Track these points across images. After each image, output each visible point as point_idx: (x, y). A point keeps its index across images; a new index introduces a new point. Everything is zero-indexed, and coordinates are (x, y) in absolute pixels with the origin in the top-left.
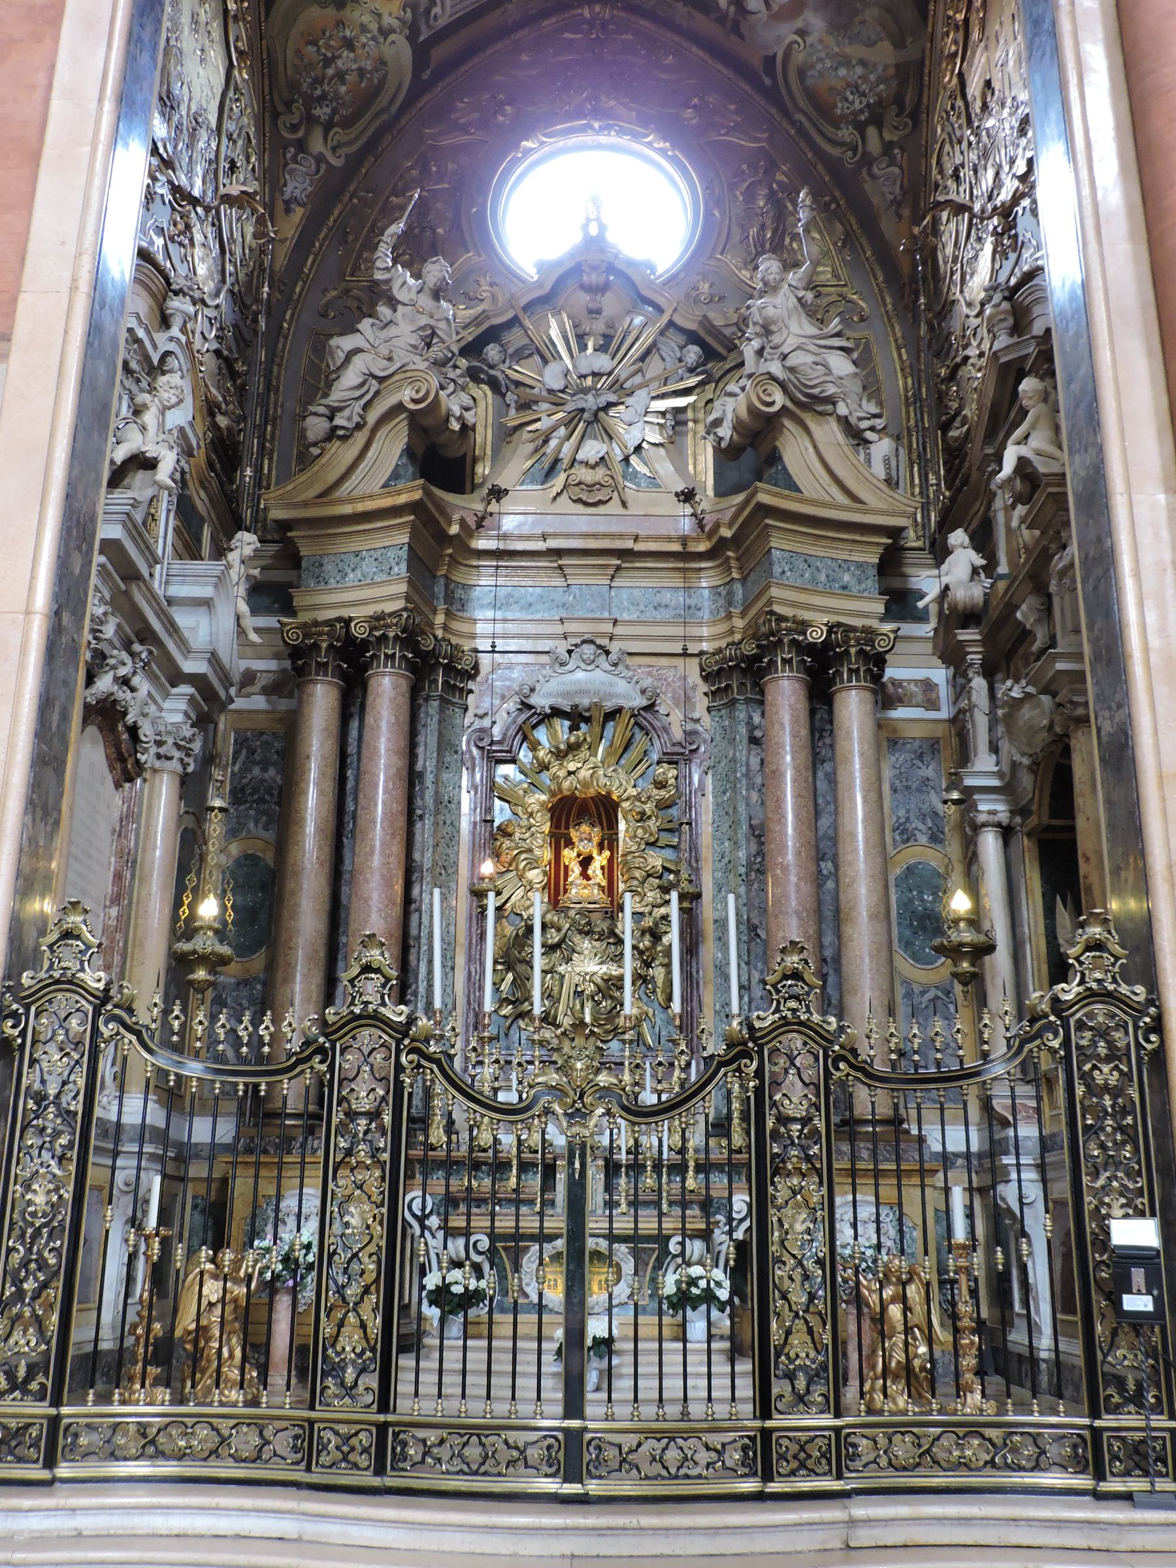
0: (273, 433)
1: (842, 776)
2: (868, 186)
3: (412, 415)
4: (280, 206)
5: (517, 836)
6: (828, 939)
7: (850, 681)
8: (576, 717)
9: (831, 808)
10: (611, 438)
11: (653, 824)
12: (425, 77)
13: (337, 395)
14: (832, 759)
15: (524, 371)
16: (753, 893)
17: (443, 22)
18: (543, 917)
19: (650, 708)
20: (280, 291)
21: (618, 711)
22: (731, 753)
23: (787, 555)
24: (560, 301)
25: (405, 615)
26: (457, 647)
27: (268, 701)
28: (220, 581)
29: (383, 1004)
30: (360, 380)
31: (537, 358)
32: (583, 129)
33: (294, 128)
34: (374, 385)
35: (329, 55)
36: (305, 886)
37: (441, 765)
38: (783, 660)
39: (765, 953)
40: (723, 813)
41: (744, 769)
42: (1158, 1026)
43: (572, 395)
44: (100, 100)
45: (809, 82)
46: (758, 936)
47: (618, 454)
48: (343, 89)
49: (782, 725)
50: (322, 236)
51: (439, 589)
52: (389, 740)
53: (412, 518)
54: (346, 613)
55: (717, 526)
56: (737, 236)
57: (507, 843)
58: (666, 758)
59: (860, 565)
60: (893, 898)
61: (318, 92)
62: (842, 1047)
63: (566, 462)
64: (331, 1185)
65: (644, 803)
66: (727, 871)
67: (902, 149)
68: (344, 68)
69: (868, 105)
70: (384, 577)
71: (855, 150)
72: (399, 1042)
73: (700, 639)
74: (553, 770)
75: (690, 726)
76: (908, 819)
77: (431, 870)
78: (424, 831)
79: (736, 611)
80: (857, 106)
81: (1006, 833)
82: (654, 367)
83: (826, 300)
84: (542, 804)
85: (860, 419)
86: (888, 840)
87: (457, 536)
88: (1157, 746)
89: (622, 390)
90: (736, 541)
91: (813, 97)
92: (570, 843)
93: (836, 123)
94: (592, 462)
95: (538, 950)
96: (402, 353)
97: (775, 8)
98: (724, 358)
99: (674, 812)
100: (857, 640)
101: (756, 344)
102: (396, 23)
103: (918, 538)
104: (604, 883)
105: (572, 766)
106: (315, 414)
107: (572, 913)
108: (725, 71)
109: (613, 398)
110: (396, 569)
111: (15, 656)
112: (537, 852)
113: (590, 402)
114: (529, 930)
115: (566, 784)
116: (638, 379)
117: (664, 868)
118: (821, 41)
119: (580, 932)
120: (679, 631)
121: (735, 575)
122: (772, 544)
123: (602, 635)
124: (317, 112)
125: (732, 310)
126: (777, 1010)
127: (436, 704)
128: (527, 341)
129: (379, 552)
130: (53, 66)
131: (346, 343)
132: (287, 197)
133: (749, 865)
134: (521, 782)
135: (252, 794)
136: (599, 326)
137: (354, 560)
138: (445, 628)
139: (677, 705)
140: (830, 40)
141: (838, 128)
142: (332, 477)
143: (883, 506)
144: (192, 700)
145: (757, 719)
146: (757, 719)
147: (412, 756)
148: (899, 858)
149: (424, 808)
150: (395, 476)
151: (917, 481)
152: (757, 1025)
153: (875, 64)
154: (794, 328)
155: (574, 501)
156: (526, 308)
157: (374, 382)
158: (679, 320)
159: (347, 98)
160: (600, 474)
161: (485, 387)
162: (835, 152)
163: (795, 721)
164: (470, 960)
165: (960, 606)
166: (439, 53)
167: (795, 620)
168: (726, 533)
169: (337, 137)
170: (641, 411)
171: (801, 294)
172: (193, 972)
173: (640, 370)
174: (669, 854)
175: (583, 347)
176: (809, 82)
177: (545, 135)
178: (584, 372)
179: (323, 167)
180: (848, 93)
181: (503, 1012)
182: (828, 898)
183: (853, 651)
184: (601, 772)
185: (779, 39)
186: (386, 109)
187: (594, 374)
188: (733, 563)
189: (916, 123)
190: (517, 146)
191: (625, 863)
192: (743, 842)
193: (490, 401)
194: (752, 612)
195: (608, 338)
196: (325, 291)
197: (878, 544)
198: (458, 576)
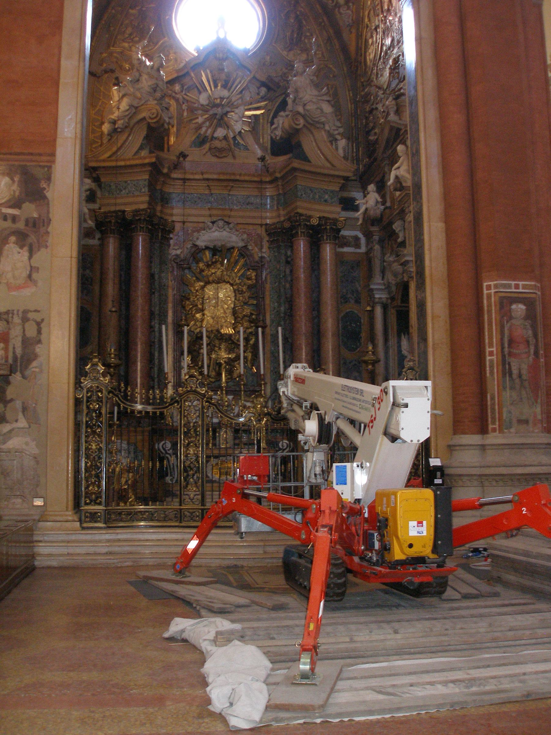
2: (338, 16)
5: (192, 299)
7: (327, 240)
8: (215, 251)
10: (228, 127)
11: (247, 295)
15: (192, 95)
22: (278, 267)
25: (149, 211)
29: (197, 387)
31: (196, 90)
38: (301, 232)
43: (212, 107)
47: (231, 135)
49: (300, 259)
54: (122, 208)
57: (187, 302)
59: (332, 192)
60: (340, 325)
63: (210, 137)
65: (243, 286)
73: (266, 218)
85: (334, 130)
88: (432, 306)
90: (283, 178)
105: (213, 271)
109: (229, 109)
110: (143, 190)
113: (219, 111)
119: (218, 339)
123: (225, 216)
127: (158, 245)
133: (285, 313)
136: (223, 77)
138: (161, 212)
139: (256, 246)
145: (289, 253)
146: (289, 253)
151: (355, 150)
160: (224, 144)
163: (305, 257)
168: (278, 175)
170: (241, 115)
171: (312, 78)
175: (216, 86)
178: (216, 97)
184: (225, 273)
188: (280, 187)
196: (101, 53)
197: (339, 183)
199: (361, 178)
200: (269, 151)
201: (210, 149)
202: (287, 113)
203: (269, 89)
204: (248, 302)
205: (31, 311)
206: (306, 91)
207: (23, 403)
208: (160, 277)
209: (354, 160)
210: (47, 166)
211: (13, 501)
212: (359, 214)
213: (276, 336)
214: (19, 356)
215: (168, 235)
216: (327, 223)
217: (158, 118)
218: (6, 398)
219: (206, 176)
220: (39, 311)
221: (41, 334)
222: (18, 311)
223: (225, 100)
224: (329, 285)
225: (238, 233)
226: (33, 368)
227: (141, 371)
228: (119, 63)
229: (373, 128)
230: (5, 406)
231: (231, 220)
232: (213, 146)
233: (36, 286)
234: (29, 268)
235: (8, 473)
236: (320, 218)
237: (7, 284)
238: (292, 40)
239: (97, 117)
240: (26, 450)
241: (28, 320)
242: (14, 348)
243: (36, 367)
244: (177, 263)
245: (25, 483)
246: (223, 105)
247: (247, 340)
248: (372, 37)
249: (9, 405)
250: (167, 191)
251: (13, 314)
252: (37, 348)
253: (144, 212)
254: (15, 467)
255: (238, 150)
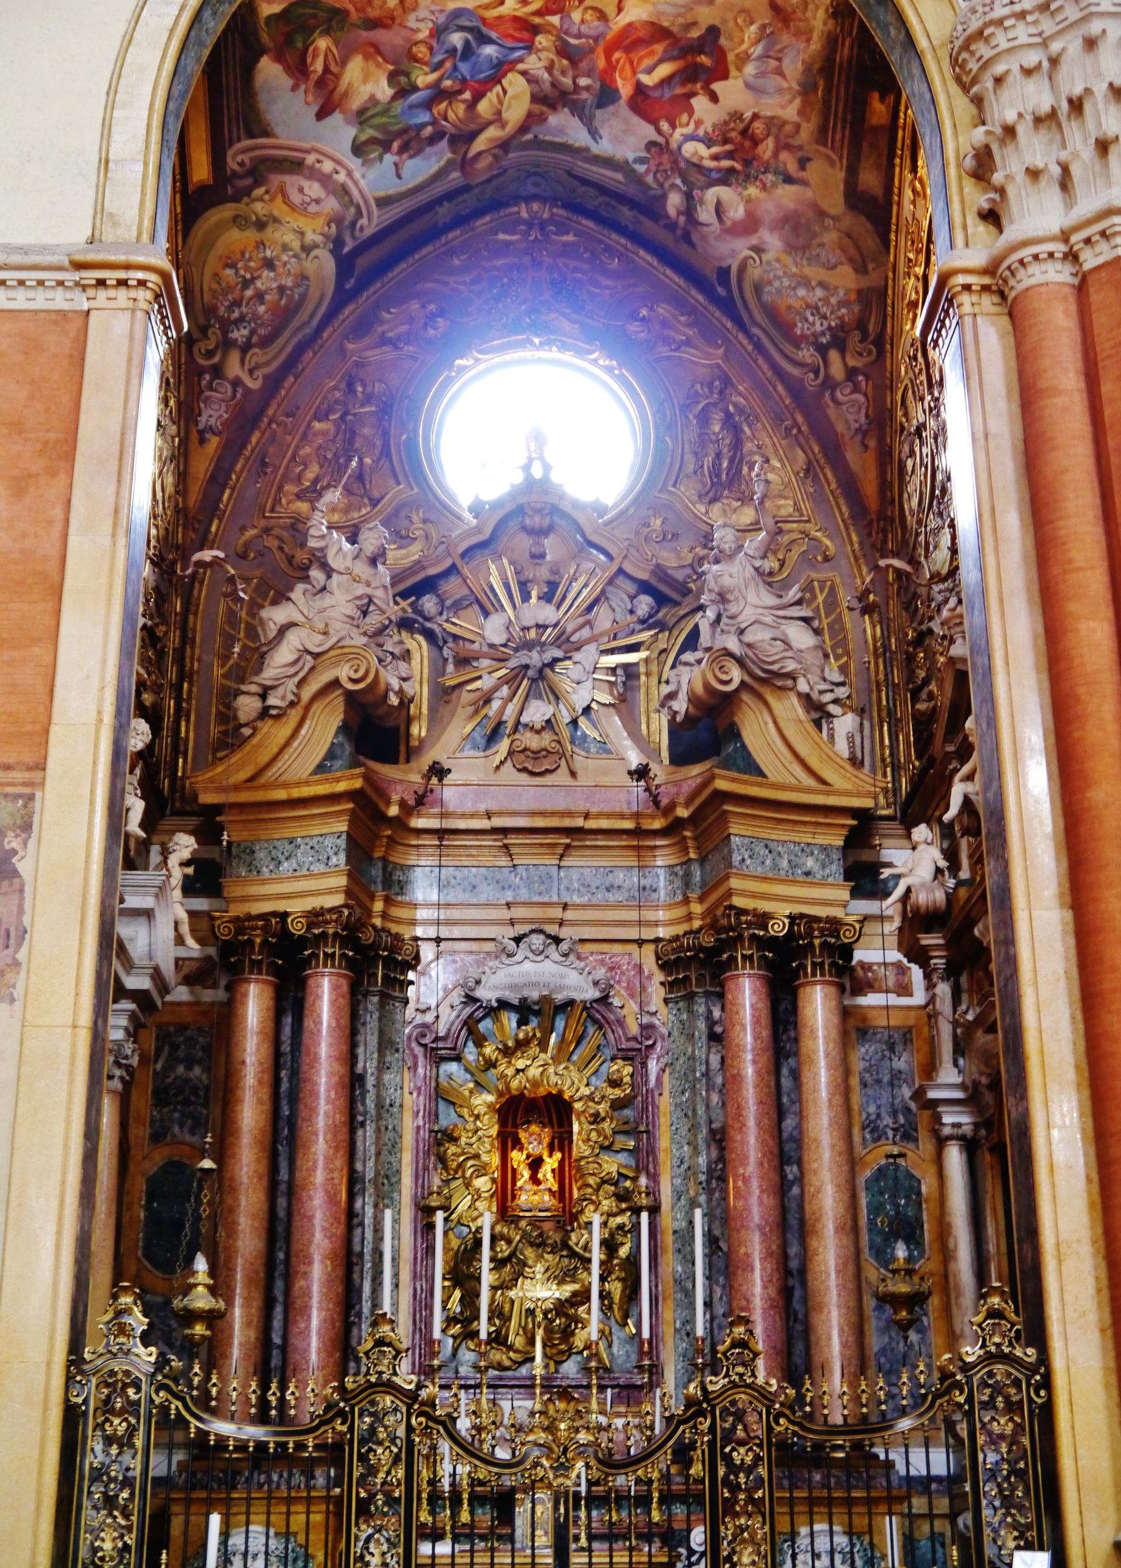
0: (190, 691)
1: (806, 1077)
2: (832, 411)
3: (350, 696)
4: (194, 437)
5: (463, 1140)
6: (793, 1250)
7: (814, 974)
8: (524, 1010)
9: (796, 1107)
10: (557, 698)
11: (608, 1127)
12: (348, 286)
13: (268, 674)
14: (796, 1054)
15: (464, 624)
16: (714, 1203)
17: (369, 232)
18: (492, 1228)
19: (604, 1000)
20: (194, 530)
21: (571, 1003)
22: (690, 1050)
23: (747, 841)
24: (502, 544)
25: (346, 912)
26: (397, 937)
27: (192, 993)
28: (161, 891)
30: (295, 656)
31: (476, 607)
32: (521, 345)
33: (210, 354)
34: (309, 661)
35: (248, 276)
36: (243, 1201)
37: (382, 1067)
39: (727, 1266)
40: (679, 1113)
41: (704, 1068)
42: (1047, 1383)
43: (516, 650)
44: (114, 535)
45: (766, 298)
46: (720, 1249)
47: (566, 717)
48: (262, 309)
49: (743, 1026)
50: (238, 467)
51: (377, 872)
52: (330, 1045)
53: (351, 806)
54: (281, 906)
55: (672, 806)
56: (690, 467)
57: (452, 1149)
58: (620, 1054)
59: (824, 849)
60: (863, 1201)
61: (236, 315)
62: (782, 1404)
63: (510, 725)
64: (354, 1530)
65: (599, 1103)
66: (686, 1178)
67: (867, 378)
68: (263, 288)
69: (830, 328)
70: (322, 868)
71: (817, 373)
72: (409, 1407)
73: (656, 924)
74: (502, 1068)
75: (646, 1020)
76: (878, 1116)
77: (375, 1181)
78: (367, 1138)
79: (693, 896)
80: (818, 328)
81: (970, 1146)
82: (603, 619)
83: (785, 539)
84: (490, 1106)
85: (821, 692)
86: (857, 1138)
87: (396, 819)
89: (568, 645)
90: (693, 819)
91: (771, 313)
92: (518, 1144)
93: (796, 342)
94: (538, 726)
95: (486, 1264)
96: (338, 625)
97: (729, 223)
98: (677, 604)
99: (627, 1112)
100: (822, 930)
101: (711, 614)
102: (319, 239)
103: (888, 806)
104: (555, 1188)
105: (520, 1064)
106: (248, 693)
107: (523, 1224)
108: (676, 278)
109: (559, 653)
110: (334, 860)
111: (65, 1067)
112: (485, 1158)
113: (535, 658)
114: (478, 1243)
115: (514, 1084)
116: (585, 633)
117: (619, 1174)
118: (778, 260)
119: (532, 1244)
120: (633, 915)
121: (692, 855)
122: (732, 831)
123: (551, 921)
124: (235, 335)
125: (686, 550)
126: (727, 1375)
127: (375, 999)
128: (466, 592)
129: (315, 840)
130: (69, 501)
131: (276, 615)
132: (201, 426)
133: (710, 1172)
134: (466, 1081)
135: (176, 1095)
136: (543, 573)
137: (290, 848)
138: (384, 916)
139: (632, 996)
140: (788, 260)
141: (798, 348)
142: (264, 757)
143: (848, 786)
144: (133, 1016)
146: (717, 1013)
147: (351, 1058)
148: (869, 1158)
149: (365, 1113)
150: (331, 755)
151: (887, 742)
152: (710, 1388)
153: (836, 288)
154: (752, 598)
155: (519, 770)
156: (463, 555)
157: (309, 658)
158: (628, 568)
159: (266, 317)
160: (546, 740)
161: (420, 638)
162: (795, 372)
163: (756, 1021)
164: (415, 1277)
165: (923, 909)
166: (362, 263)
167: (754, 912)
168: (683, 812)
169: (255, 359)
171: (758, 563)
172: (191, 1327)
173: (589, 623)
174: (623, 1158)
175: (526, 597)
176: (766, 298)
177: (480, 352)
178: (527, 624)
179: (240, 390)
180: (808, 314)
181: (452, 1332)
182: (793, 1205)
183: (817, 942)
184: (551, 1070)
185: (734, 253)
186: (308, 322)
187: (538, 626)
188: (690, 843)
189: (881, 353)
190: (452, 365)
191: (579, 1169)
192: (702, 1147)
193: (425, 654)
194: (713, 898)
195: (553, 585)
196: (243, 529)
197: (843, 826)
198: (396, 858)
199: (904, 811)
200: (665, 754)
201: (511, 753)
202: (699, 654)
203: (661, 600)
204: (612, 1144)
206: (745, 598)
208: (378, 1085)
209: (885, 767)
210: (21, 796)
212: (890, 905)
213: (685, 1237)
215: (404, 972)
216: (813, 930)
217: (369, 680)
219: (498, 822)
223: (549, 630)
224: (824, 1094)
225: (582, 964)
227: (319, 1333)
228: (286, 549)
229: (926, 682)
231: (565, 932)
232: (519, 746)
236: (792, 918)
238: (718, 476)
239: (228, 683)
244: (425, 1046)
246: (543, 644)
247: (610, 1246)
248: (912, 453)
250: (397, 860)
253: (334, 917)
255: (583, 753)
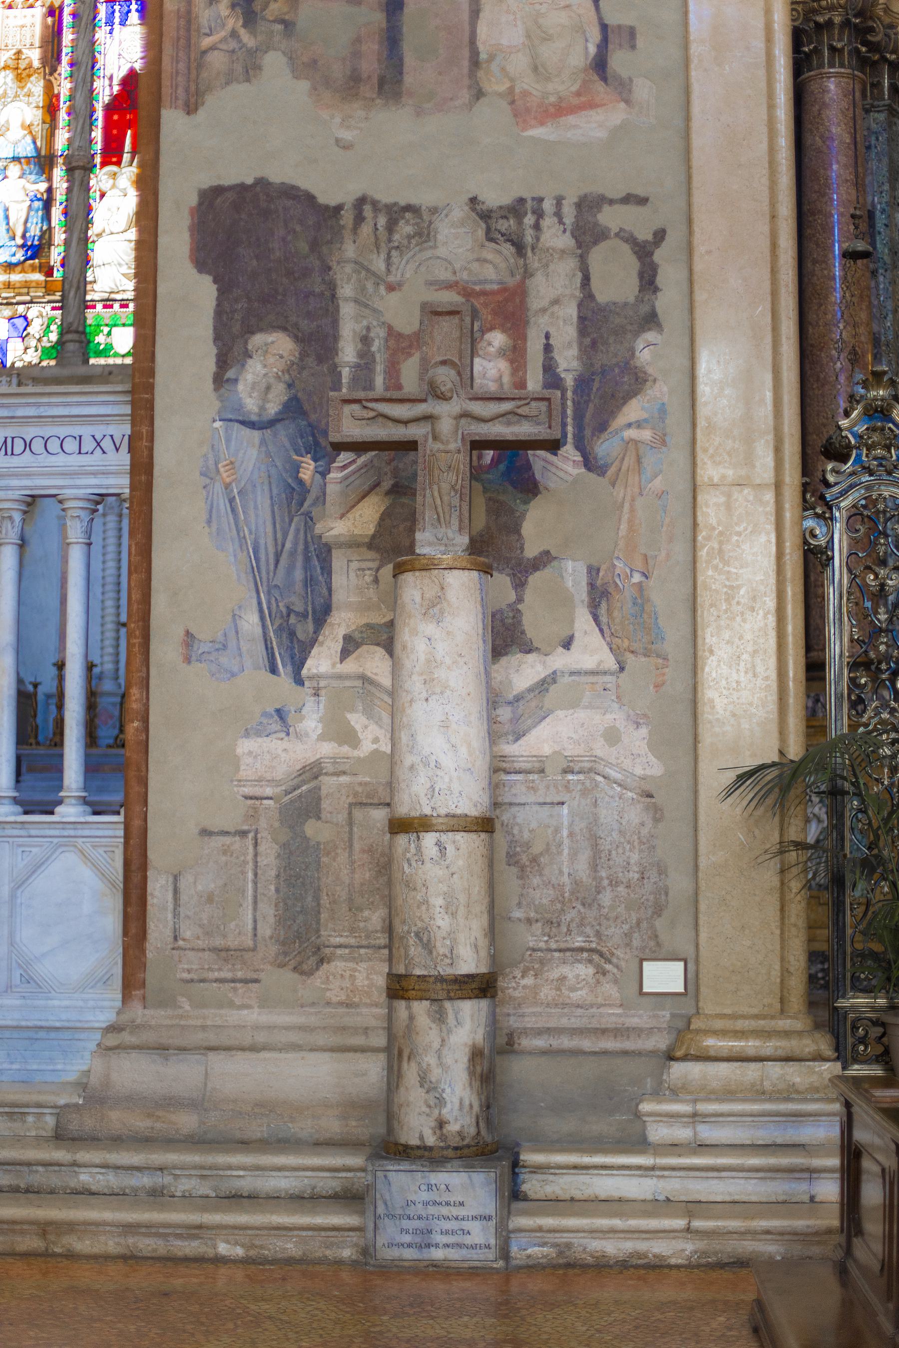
205: (611, 202)
207: (593, 571)
211: (555, 974)
214: (569, 380)
218: (522, 549)
220: (642, 201)
221: (656, 290)
222: (559, 201)
226: (629, 425)
230: (520, 585)
233: (627, 102)
234: (595, 35)
235: (534, 860)
237: (511, 97)
240: (609, 764)
241: (601, 235)
242: (548, 348)
243: (639, 425)
245: (606, 898)
249: (535, 579)
251: (539, 214)
252: (640, 344)
254: (565, 833)
